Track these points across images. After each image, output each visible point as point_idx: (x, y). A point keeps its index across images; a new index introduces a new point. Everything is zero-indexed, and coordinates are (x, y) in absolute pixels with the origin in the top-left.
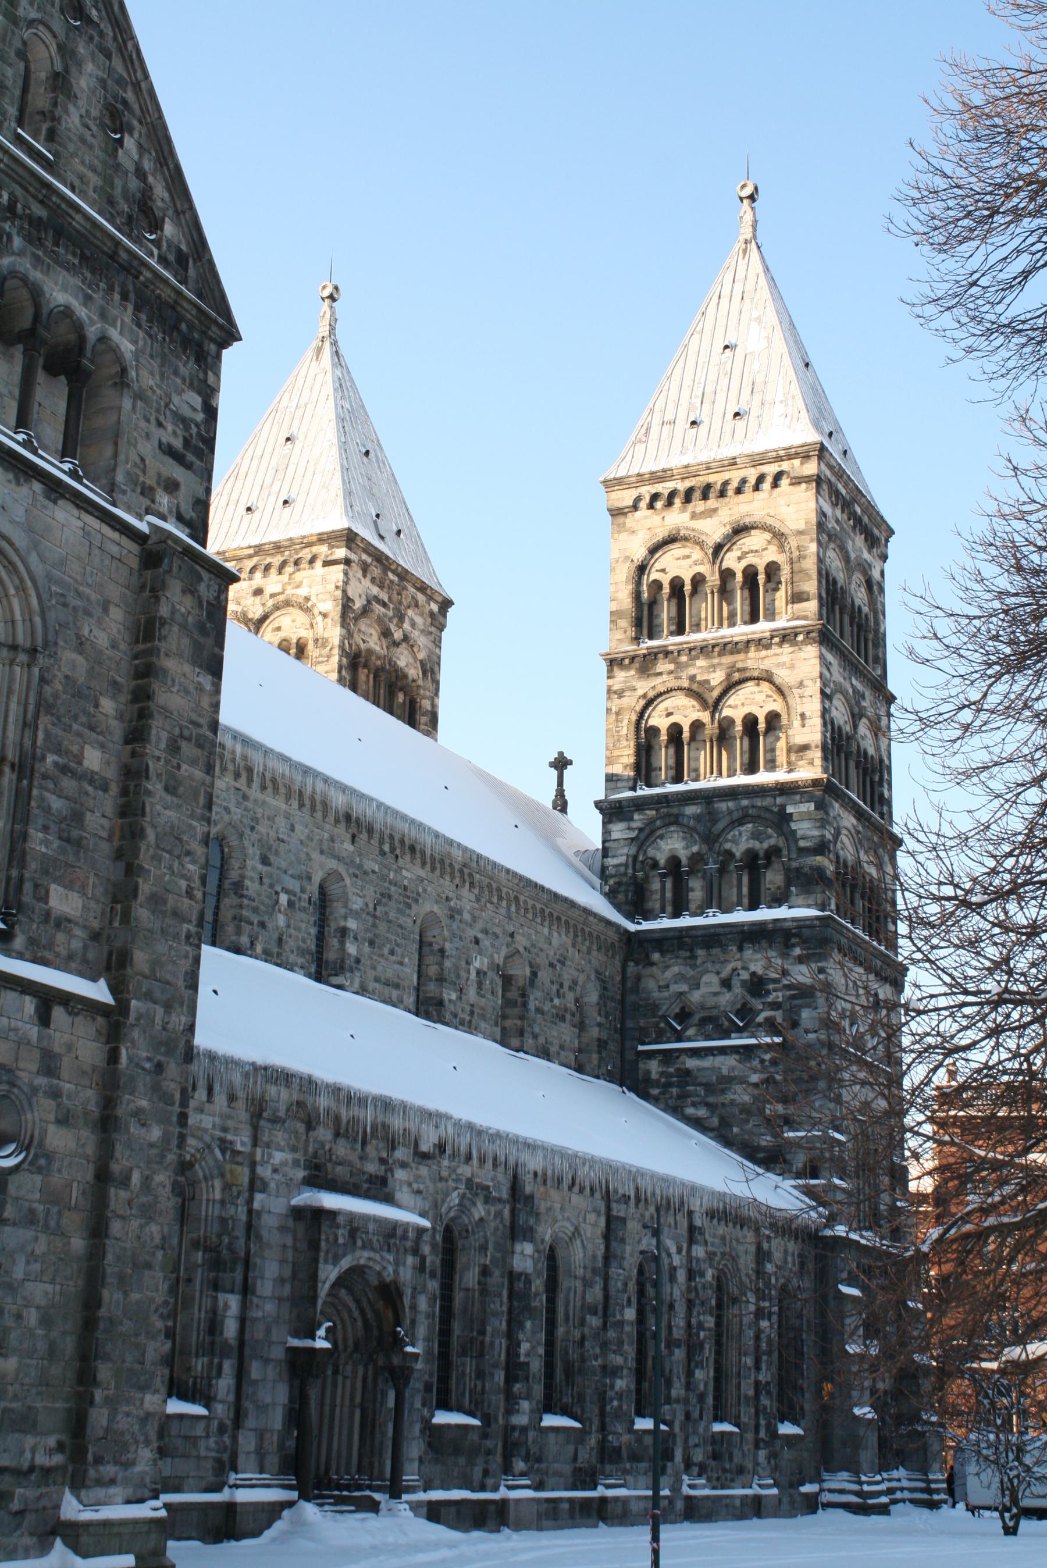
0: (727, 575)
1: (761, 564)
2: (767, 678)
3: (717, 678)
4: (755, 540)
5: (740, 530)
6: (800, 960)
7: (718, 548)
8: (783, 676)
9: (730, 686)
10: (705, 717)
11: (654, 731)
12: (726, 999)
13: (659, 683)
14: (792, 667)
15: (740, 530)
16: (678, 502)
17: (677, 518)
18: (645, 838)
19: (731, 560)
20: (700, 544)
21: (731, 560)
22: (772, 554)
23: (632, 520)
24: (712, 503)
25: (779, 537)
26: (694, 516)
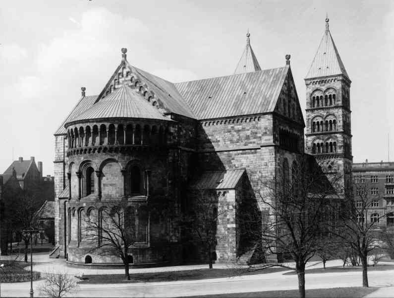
0: (326, 96)
1: (332, 94)
2: (334, 115)
3: (325, 114)
4: (331, 91)
5: (328, 89)
6: (340, 160)
7: (325, 91)
8: (336, 114)
9: (327, 116)
10: (323, 120)
11: (314, 123)
12: (328, 166)
13: (316, 115)
14: (337, 112)
15: (328, 89)
16: (317, 83)
17: (318, 86)
18: (314, 140)
19: (327, 93)
20: (321, 90)
21: (327, 93)
22: (334, 93)
23: (309, 86)
24: (323, 84)
25: (335, 90)
26: (320, 86)
